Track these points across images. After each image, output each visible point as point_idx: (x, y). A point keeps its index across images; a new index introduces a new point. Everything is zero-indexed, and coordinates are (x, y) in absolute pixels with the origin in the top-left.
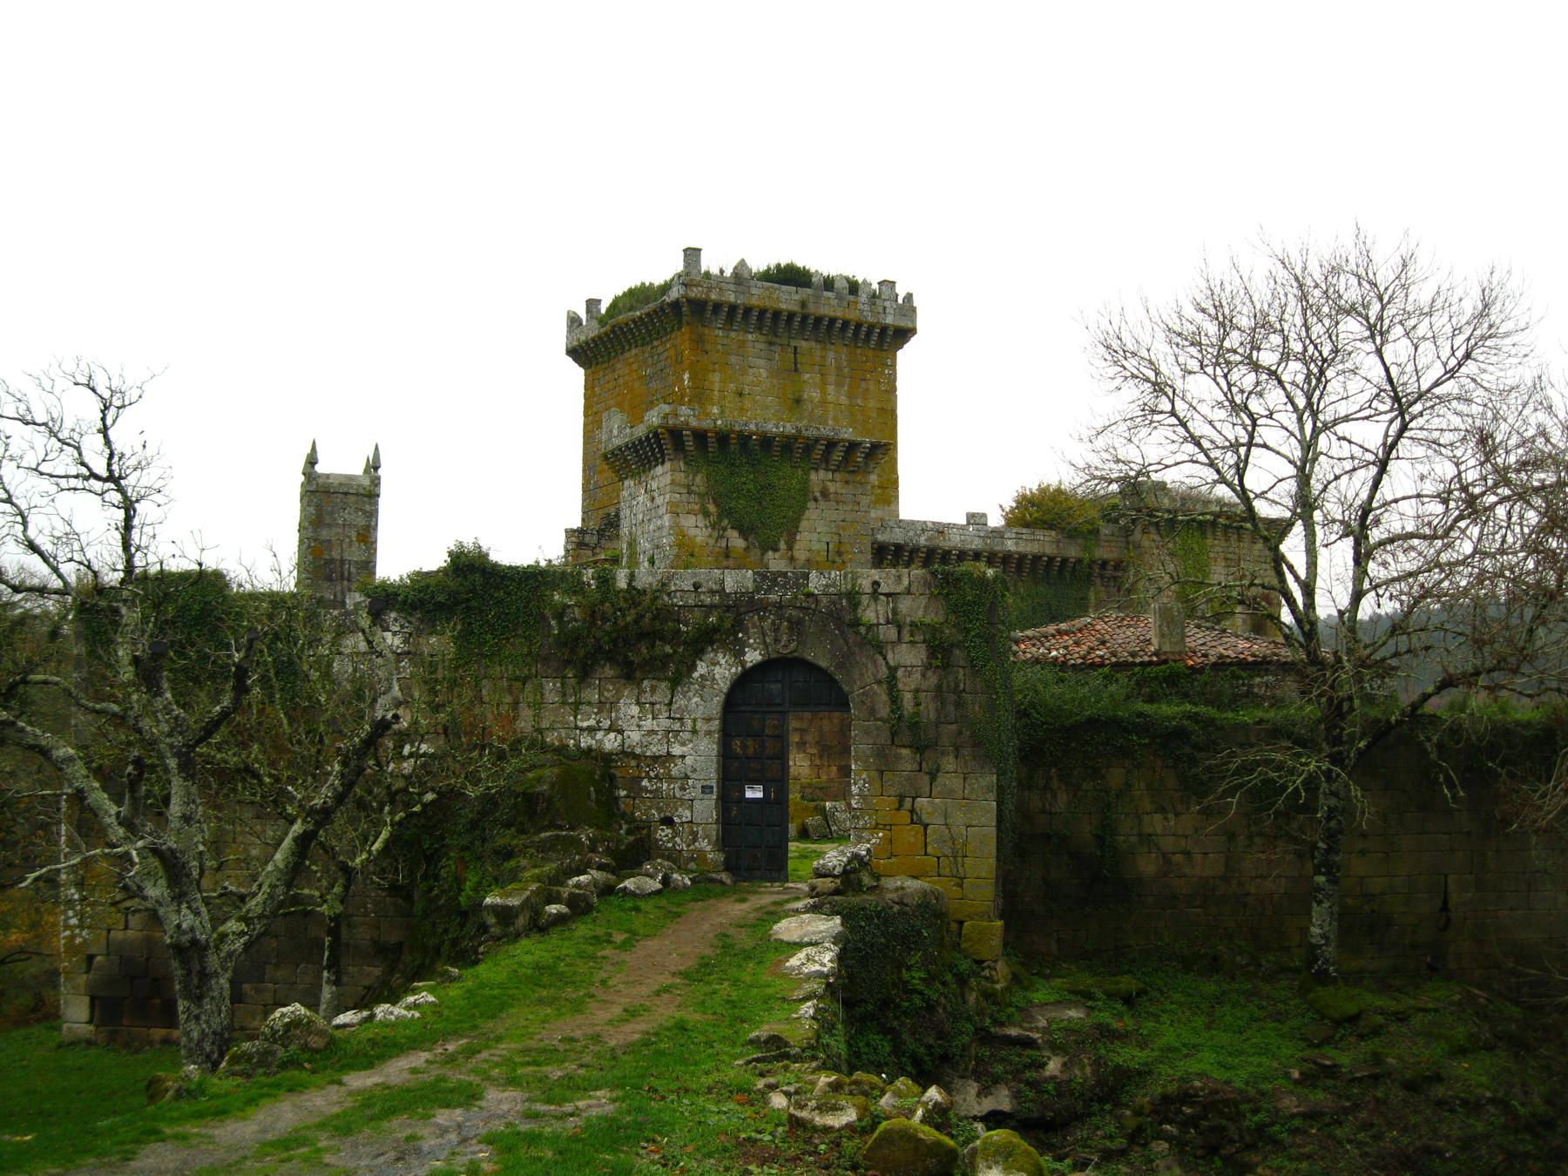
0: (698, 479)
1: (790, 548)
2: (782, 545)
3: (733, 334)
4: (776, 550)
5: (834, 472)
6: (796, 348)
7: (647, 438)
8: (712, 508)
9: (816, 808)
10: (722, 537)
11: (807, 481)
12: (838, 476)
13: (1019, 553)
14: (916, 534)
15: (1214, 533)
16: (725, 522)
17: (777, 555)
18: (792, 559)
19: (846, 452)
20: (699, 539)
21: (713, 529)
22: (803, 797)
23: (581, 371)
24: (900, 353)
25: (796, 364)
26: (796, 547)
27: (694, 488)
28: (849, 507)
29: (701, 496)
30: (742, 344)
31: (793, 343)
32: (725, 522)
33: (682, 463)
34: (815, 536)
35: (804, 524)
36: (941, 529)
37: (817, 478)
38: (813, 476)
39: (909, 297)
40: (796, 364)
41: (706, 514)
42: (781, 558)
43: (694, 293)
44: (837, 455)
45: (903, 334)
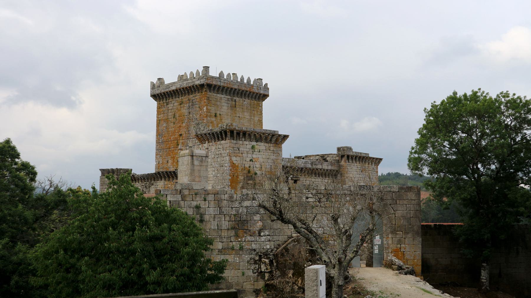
3: (218, 95)
6: (235, 100)
7: (221, 132)
19: (271, 138)
24: (263, 102)
25: (235, 105)
30: (221, 98)
31: (235, 98)
34: (268, 164)
39: (266, 84)
40: (235, 105)
43: (209, 82)
44: (274, 139)
45: (265, 96)
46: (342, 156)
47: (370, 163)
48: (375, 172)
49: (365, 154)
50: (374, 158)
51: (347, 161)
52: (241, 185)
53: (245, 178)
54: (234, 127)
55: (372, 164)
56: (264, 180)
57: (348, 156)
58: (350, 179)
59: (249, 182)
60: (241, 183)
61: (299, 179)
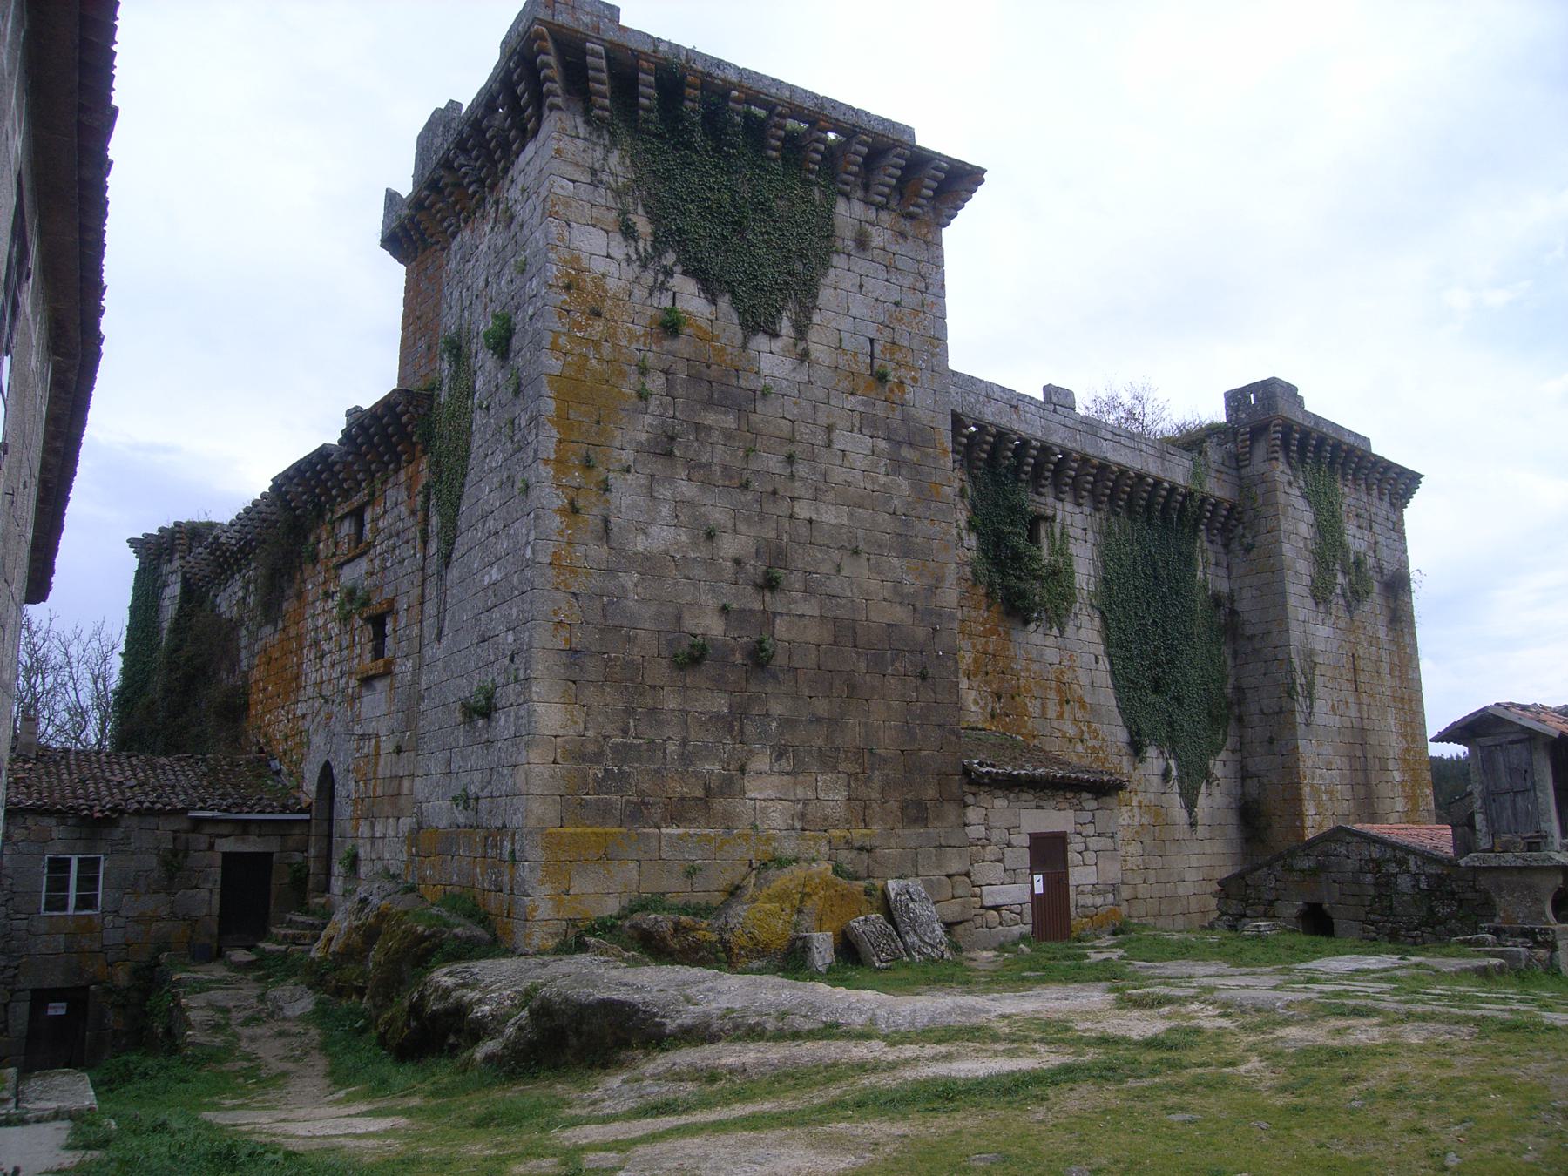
0: (614, 158)
1: (801, 332)
2: (786, 327)
4: (775, 335)
5: (880, 207)
8: (643, 225)
9: (868, 892)
10: (663, 288)
11: (829, 214)
12: (884, 215)
13: (1119, 465)
14: (978, 402)
15: (1344, 477)
16: (670, 258)
17: (777, 345)
18: (804, 356)
20: (611, 284)
21: (644, 267)
22: (837, 870)
23: (403, 268)
26: (813, 335)
27: (605, 178)
28: (908, 281)
29: (618, 193)
32: (670, 258)
33: (579, 121)
35: (826, 296)
36: (1015, 401)
37: (848, 213)
38: (841, 206)
41: (628, 232)
42: (785, 352)
44: (888, 175)
46: (1258, 431)
47: (1375, 493)
48: (1395, 536)
49: (1357, 436)
50: (1389, 466)
51: (1280, 455)
52: (642, 429)
53: (680, 390)
54: (586, 19)
55: (1381, 493)
56: (823, 420)
57: (1288, 428)
58: (1301, 545)
59: (710, 418)
60: (649, 419)
61: (1049, 513)
